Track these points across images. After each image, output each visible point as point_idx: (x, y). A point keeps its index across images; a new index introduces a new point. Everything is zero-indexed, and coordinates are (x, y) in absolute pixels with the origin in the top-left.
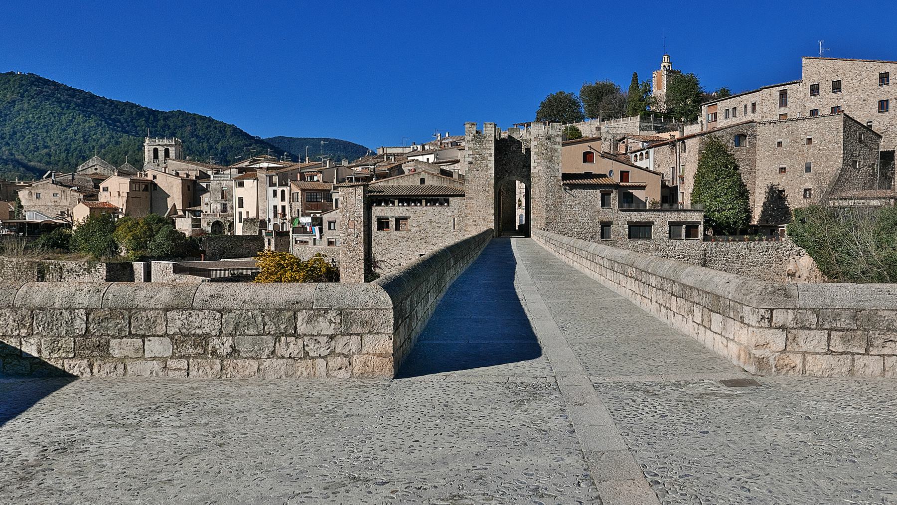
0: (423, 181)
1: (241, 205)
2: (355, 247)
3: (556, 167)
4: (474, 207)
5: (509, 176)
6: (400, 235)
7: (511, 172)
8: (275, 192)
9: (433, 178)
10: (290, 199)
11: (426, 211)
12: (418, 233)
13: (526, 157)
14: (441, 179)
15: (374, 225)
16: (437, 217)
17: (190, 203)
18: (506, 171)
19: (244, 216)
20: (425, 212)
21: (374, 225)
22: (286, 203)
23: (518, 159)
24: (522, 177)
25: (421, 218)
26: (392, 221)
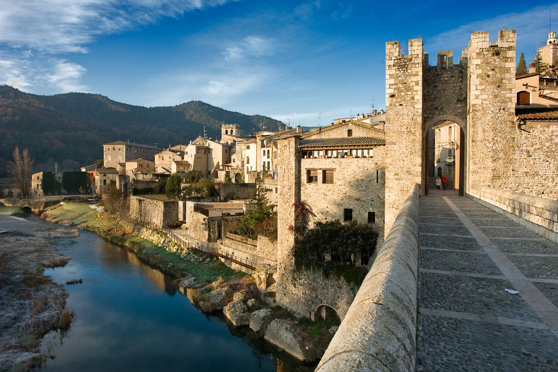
0: (350, 132)
1: (248, 163)
2: (288, 199)
3: (508, 95)
5: (439, 115)
6: (326, 188)
7: (442, 109)
8: (264, 151)
9: (359, 129)
10: (272, 156)
11: (350, 163)
12: (343, 186)
13: (461, 89)
14: (367, 131)
15: (304, 178)
17: (227, 161)
18: (436, 108)
19: (250, 170)
20: (350, 164)
21: (304, 178)
22: (270, 160)
23: (451, 92)
24: (456, 115)
25: (346, 170)
26: (320, 173)
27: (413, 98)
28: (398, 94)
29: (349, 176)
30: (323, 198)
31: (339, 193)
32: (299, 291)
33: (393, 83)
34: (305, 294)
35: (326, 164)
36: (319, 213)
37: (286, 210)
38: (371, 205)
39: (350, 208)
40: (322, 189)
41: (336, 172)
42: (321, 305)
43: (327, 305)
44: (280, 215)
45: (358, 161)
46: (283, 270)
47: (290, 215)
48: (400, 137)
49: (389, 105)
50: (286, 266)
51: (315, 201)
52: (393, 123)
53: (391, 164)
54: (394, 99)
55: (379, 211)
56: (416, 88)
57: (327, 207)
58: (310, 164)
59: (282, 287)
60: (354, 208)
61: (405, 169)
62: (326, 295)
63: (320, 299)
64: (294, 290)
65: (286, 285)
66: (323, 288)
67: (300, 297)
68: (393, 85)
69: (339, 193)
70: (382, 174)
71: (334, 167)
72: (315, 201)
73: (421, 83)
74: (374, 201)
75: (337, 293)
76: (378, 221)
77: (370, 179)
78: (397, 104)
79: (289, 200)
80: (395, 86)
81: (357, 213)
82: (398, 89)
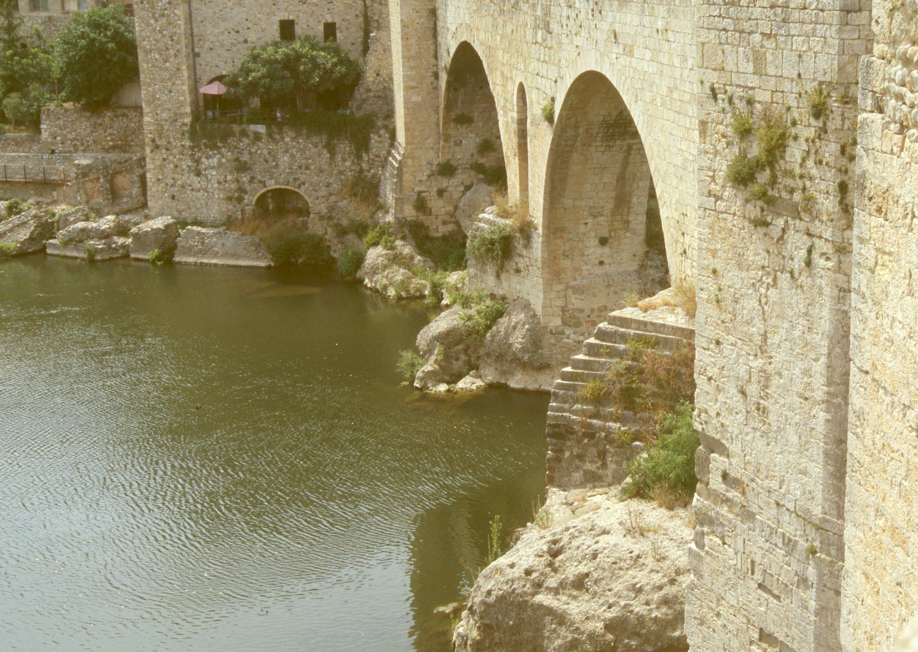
32: (208, 181)
34: (226, 182)
36: (232, 32)
39: (291, 18)
42: (264, 190)
43: (278, 187)
44: (145, 43)
47: (172, 40)
51: (221, 10)
55: (343, 20)
57: (247, 20)
60: (298, 17)
62: (274, 170)
63: (260, 182)
64: (196, 182)
65: (173, 179)
67: (212, 190)
72: (221, 10)
75: (295, 162)
79: (166, 12)
81: (304, 26)
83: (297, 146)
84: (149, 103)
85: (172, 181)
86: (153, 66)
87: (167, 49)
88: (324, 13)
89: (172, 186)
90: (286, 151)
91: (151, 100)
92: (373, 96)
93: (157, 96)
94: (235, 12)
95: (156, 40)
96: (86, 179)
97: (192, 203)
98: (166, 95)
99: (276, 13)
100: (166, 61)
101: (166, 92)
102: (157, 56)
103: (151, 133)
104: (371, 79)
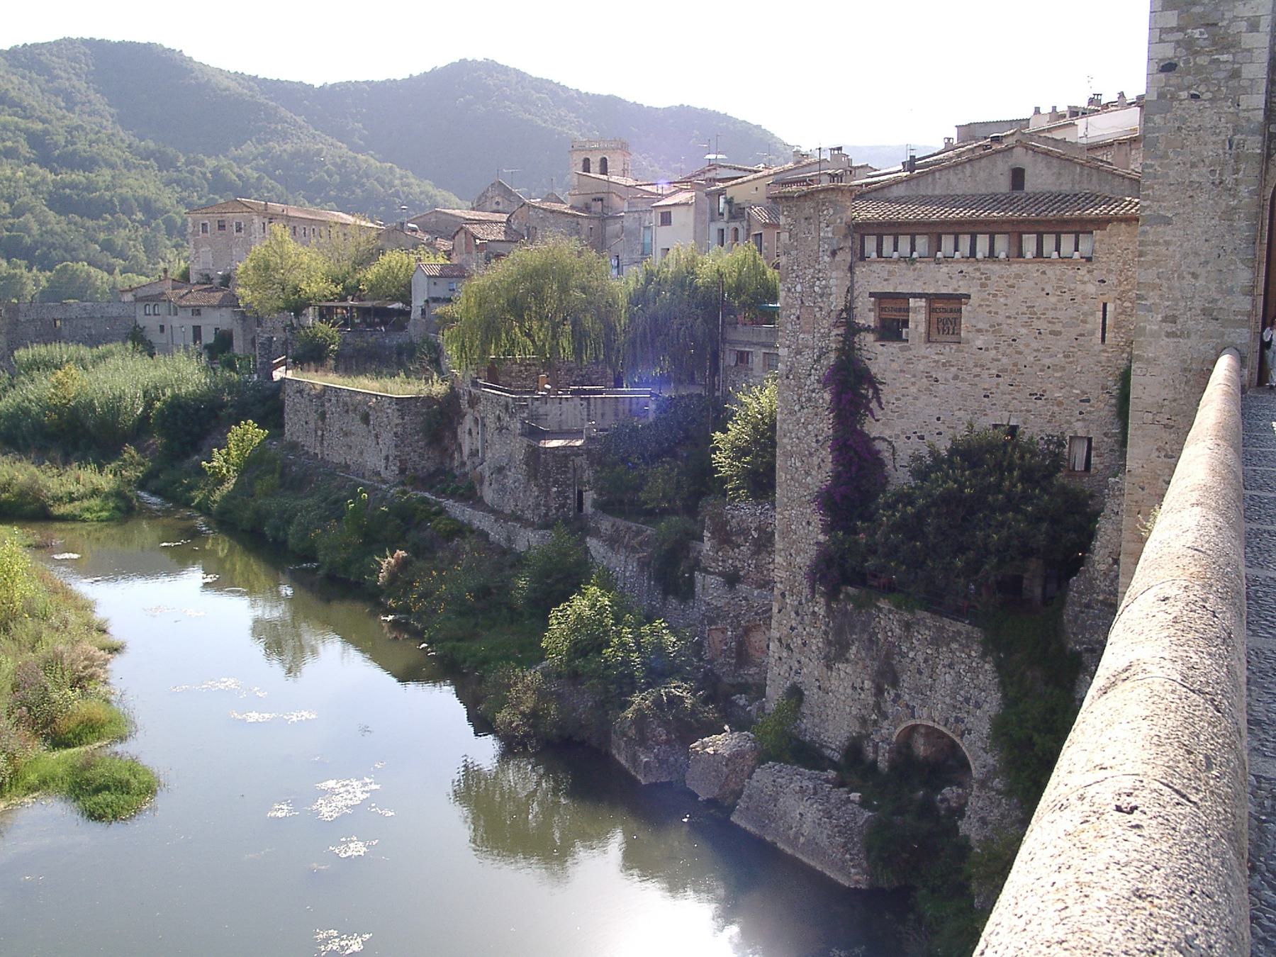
0: (1018, 176)
4: (1173, 257)
6: (936, 357)
11: (1018, 276)
16: (1053, 299)
25: (1002, 300)
26: (916, 310)
27: (1235, 74)
28: (1187, 62)
29: (1011, 321)
30: (927, 389)
31: (979, 376)
33: (1174, 24)
34: (862, 689)
35: (941, 280)
37: (805, 425)
38: (1081, 413)
40: (924, 361)
41: (969, 308)
42: (912, 722)
43: (931, 724)
44: (786, 440)
45: (1044, 273)
46: (793, 615)
48: (1187, 200)
49: (1155, 99)
50: (800, 603)
51: (897, 399)
52: (1165, 156)
53: (1154, 287)
54: (1174, 78)
55: (1106, 435)
56: (1248, 40)
58: (886, 280)
59: (786, 667)
61: (1197, 304)
63: (908, 706)
65: (799, 662)
66: (920, 673)
68: (1171, 30)
69: (979, 376)
70: (1121, 314)
71: (962, 291)
72: (897, 399)
73: (1265, 25)
74: (1088, 401)
76: (1102, 466)
77: (1078, 330)
78: (1184, 94)
79: (814, 395)
80: (1180, 36)
82: (1189, 44)
83: (968, 661)
84: (784, 535)
85: (796, 663)
86: (792, 479)
87: (811, 454)
88: (1073, 420)
89: (797, 672)
90: (951, 666)
91: (785, 530)
92: (1101, 602)
93: (793, 527)
94: (919, 404)
95: (798, 438)
96: (713, 627)
97: (816, 709)
98: (804, 528)
99: (988, 412)
100: (807, 473)
101: (804, 524)
102: (798, 464)
103: (781, 582)
104: (1103, 567)
